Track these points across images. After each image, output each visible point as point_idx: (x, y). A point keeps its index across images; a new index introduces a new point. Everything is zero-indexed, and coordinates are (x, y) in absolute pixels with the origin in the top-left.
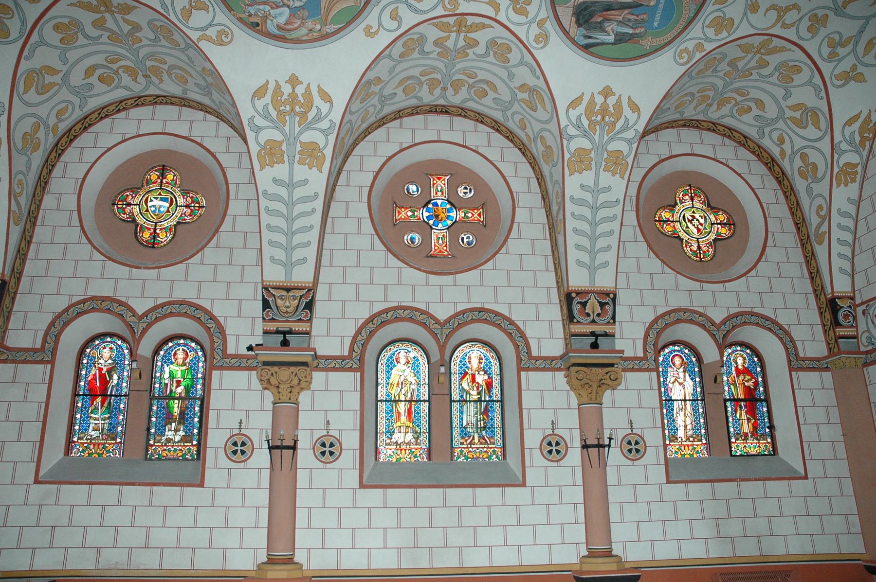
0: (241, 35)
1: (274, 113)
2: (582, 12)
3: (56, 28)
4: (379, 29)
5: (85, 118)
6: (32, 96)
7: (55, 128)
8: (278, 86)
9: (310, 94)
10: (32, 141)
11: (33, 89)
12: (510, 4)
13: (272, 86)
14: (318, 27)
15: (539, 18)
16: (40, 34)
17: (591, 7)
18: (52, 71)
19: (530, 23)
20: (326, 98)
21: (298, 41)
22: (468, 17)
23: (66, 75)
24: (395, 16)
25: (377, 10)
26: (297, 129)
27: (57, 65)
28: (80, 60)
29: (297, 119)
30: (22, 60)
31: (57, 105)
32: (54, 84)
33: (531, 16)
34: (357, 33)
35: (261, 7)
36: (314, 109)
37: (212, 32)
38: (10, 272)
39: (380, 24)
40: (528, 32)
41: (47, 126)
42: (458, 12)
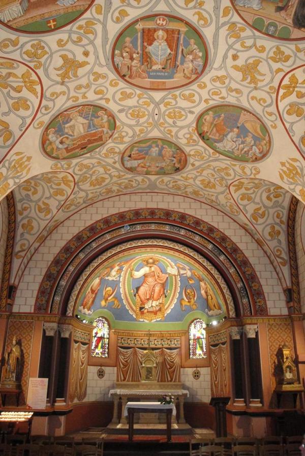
0: (258, 165)
1: (291, 180)
2: (300, 22)
3: (242, 199)
4: (274, 123)
5: (290, 210)
6: (261, 221)
7: (282, 222)
8: (282, 170)
9: (291, 164)
10: (275, 233)
11: (259, 218)
12: (281, 63)
13: (281, 172)
14: (265, 142)
15: (294, 50)
16: (241, 205)
17: (298, 16)
18: (259, 209)
19: (296, 55)
20: (296, 160)
21: (268, 151)
22: (283, 83)
23: (265, 206)
24: (271, 114)
25: (264, 118)
26: (301, 180)
27: (258, 206)
28: (261, 200)
29: (298, 176)
30: (246, 215)
31: (273, 216)
32: (264, 212)
33: (292, 54)
34: (273, 132)
35: (250, 153)
36: (298, 168)
37: (254, 172)
38: (291, 284)
39: (272, 121)
40: (300, 59)
41: (277, 224)
42: (277, 88)
